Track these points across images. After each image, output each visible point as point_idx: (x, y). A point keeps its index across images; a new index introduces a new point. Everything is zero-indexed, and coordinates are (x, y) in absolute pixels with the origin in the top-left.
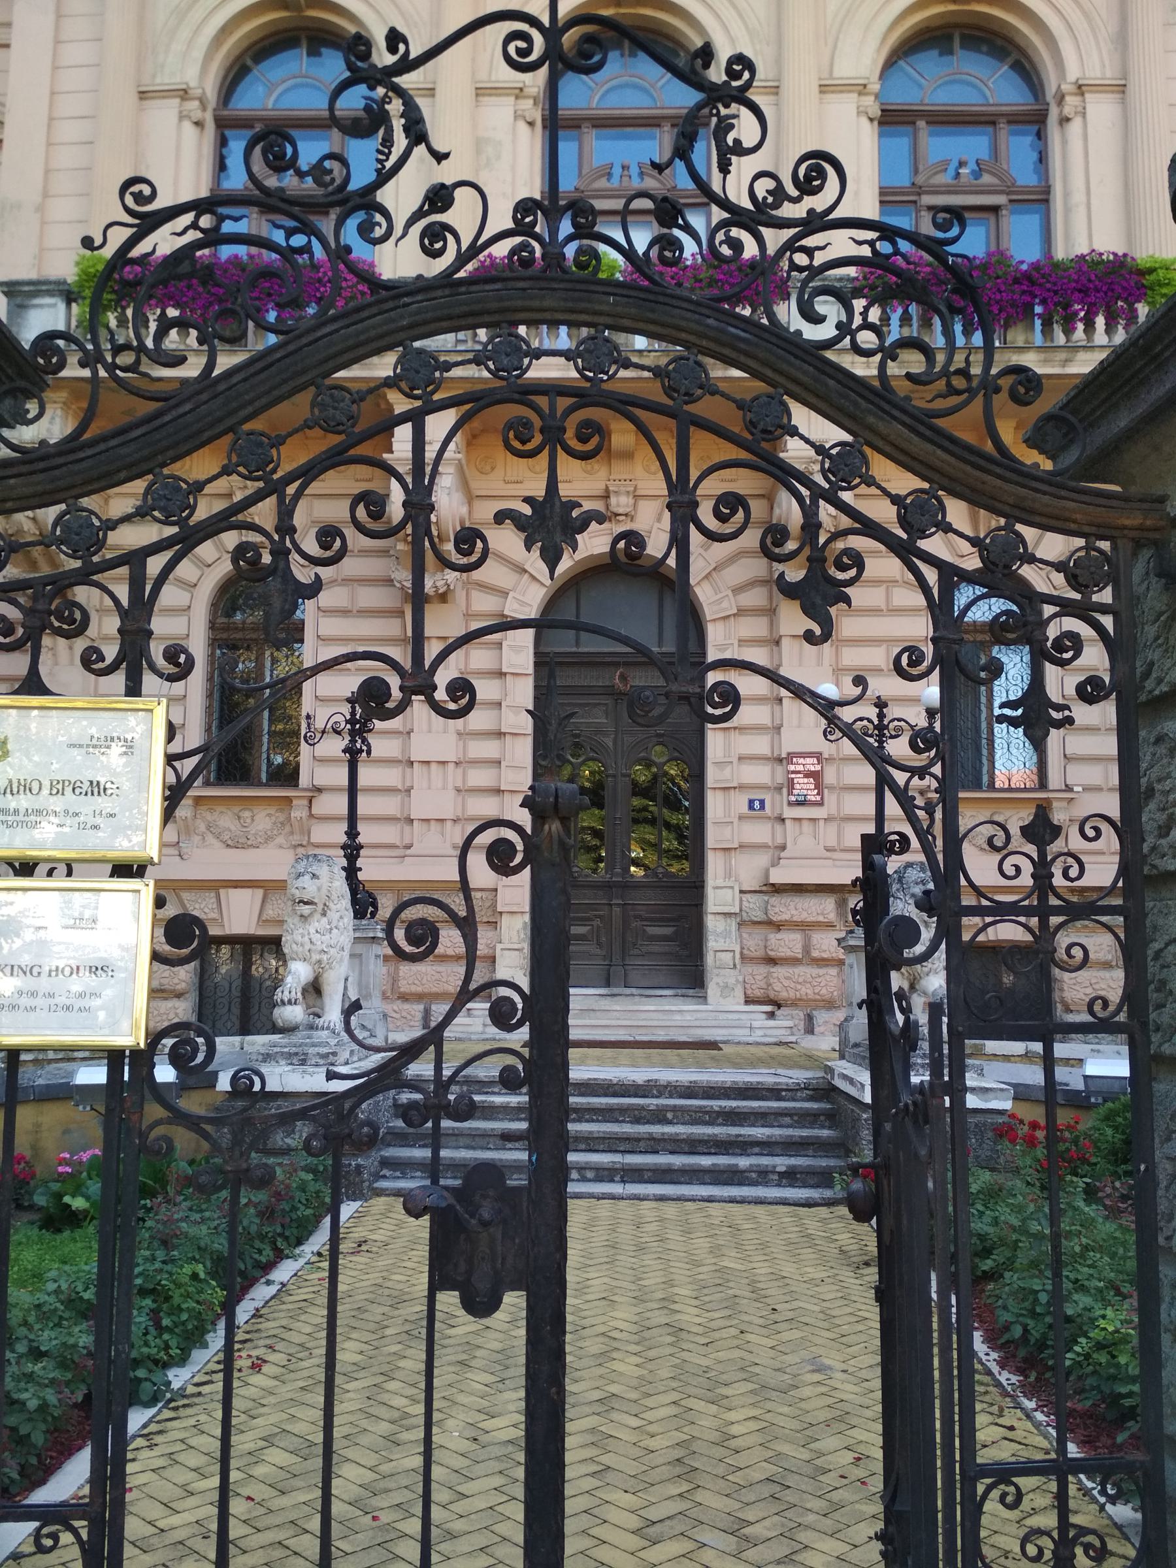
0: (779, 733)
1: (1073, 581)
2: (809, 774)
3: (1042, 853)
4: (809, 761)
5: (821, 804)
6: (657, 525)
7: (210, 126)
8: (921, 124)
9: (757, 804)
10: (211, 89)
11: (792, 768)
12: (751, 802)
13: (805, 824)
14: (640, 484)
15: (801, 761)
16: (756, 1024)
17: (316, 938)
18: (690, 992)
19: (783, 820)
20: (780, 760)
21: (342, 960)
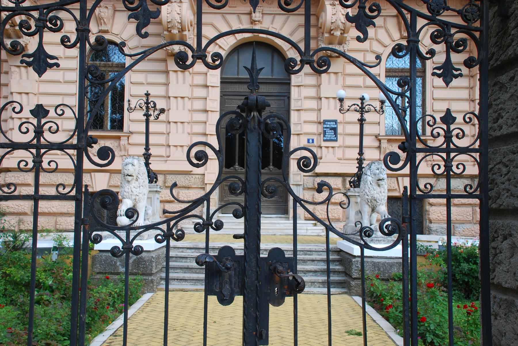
0: (320, 112)
1: (465, 18)
2: (332, 129)
3: (448, 128)
4: (332, 123)
5: (336, 140)
6: (271, 26)
9: (311, 141)
11: (325, 126)
12: (308, 140)
13: (330, 148)
15: (329, 123)
16: (309, 228)
17: (134, 190)
18: (283, 216)
19: (321, 147)
20: (320, 123)
21: (144, 199)
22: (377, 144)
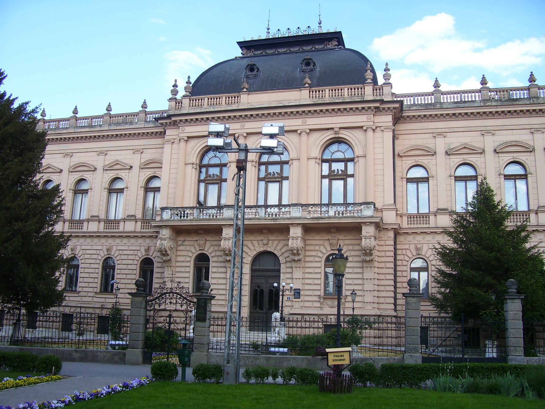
2: (297, 293)
5: (300, 298)
7: (198, 167)
8: (330, 162)
9: (289, 298)
10: (198, 162)
12: (288, 298)
14: (269, 238)
19: (293, 301)
22: (318, 300)
